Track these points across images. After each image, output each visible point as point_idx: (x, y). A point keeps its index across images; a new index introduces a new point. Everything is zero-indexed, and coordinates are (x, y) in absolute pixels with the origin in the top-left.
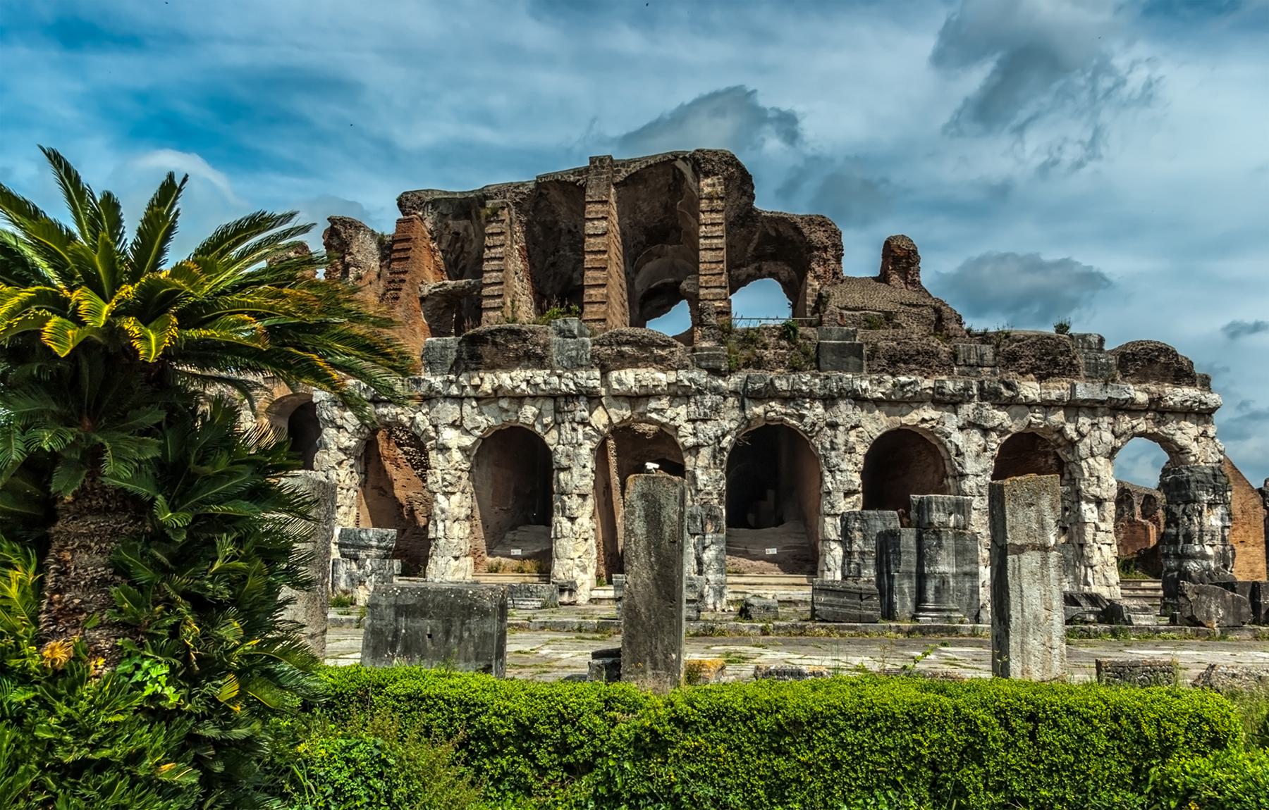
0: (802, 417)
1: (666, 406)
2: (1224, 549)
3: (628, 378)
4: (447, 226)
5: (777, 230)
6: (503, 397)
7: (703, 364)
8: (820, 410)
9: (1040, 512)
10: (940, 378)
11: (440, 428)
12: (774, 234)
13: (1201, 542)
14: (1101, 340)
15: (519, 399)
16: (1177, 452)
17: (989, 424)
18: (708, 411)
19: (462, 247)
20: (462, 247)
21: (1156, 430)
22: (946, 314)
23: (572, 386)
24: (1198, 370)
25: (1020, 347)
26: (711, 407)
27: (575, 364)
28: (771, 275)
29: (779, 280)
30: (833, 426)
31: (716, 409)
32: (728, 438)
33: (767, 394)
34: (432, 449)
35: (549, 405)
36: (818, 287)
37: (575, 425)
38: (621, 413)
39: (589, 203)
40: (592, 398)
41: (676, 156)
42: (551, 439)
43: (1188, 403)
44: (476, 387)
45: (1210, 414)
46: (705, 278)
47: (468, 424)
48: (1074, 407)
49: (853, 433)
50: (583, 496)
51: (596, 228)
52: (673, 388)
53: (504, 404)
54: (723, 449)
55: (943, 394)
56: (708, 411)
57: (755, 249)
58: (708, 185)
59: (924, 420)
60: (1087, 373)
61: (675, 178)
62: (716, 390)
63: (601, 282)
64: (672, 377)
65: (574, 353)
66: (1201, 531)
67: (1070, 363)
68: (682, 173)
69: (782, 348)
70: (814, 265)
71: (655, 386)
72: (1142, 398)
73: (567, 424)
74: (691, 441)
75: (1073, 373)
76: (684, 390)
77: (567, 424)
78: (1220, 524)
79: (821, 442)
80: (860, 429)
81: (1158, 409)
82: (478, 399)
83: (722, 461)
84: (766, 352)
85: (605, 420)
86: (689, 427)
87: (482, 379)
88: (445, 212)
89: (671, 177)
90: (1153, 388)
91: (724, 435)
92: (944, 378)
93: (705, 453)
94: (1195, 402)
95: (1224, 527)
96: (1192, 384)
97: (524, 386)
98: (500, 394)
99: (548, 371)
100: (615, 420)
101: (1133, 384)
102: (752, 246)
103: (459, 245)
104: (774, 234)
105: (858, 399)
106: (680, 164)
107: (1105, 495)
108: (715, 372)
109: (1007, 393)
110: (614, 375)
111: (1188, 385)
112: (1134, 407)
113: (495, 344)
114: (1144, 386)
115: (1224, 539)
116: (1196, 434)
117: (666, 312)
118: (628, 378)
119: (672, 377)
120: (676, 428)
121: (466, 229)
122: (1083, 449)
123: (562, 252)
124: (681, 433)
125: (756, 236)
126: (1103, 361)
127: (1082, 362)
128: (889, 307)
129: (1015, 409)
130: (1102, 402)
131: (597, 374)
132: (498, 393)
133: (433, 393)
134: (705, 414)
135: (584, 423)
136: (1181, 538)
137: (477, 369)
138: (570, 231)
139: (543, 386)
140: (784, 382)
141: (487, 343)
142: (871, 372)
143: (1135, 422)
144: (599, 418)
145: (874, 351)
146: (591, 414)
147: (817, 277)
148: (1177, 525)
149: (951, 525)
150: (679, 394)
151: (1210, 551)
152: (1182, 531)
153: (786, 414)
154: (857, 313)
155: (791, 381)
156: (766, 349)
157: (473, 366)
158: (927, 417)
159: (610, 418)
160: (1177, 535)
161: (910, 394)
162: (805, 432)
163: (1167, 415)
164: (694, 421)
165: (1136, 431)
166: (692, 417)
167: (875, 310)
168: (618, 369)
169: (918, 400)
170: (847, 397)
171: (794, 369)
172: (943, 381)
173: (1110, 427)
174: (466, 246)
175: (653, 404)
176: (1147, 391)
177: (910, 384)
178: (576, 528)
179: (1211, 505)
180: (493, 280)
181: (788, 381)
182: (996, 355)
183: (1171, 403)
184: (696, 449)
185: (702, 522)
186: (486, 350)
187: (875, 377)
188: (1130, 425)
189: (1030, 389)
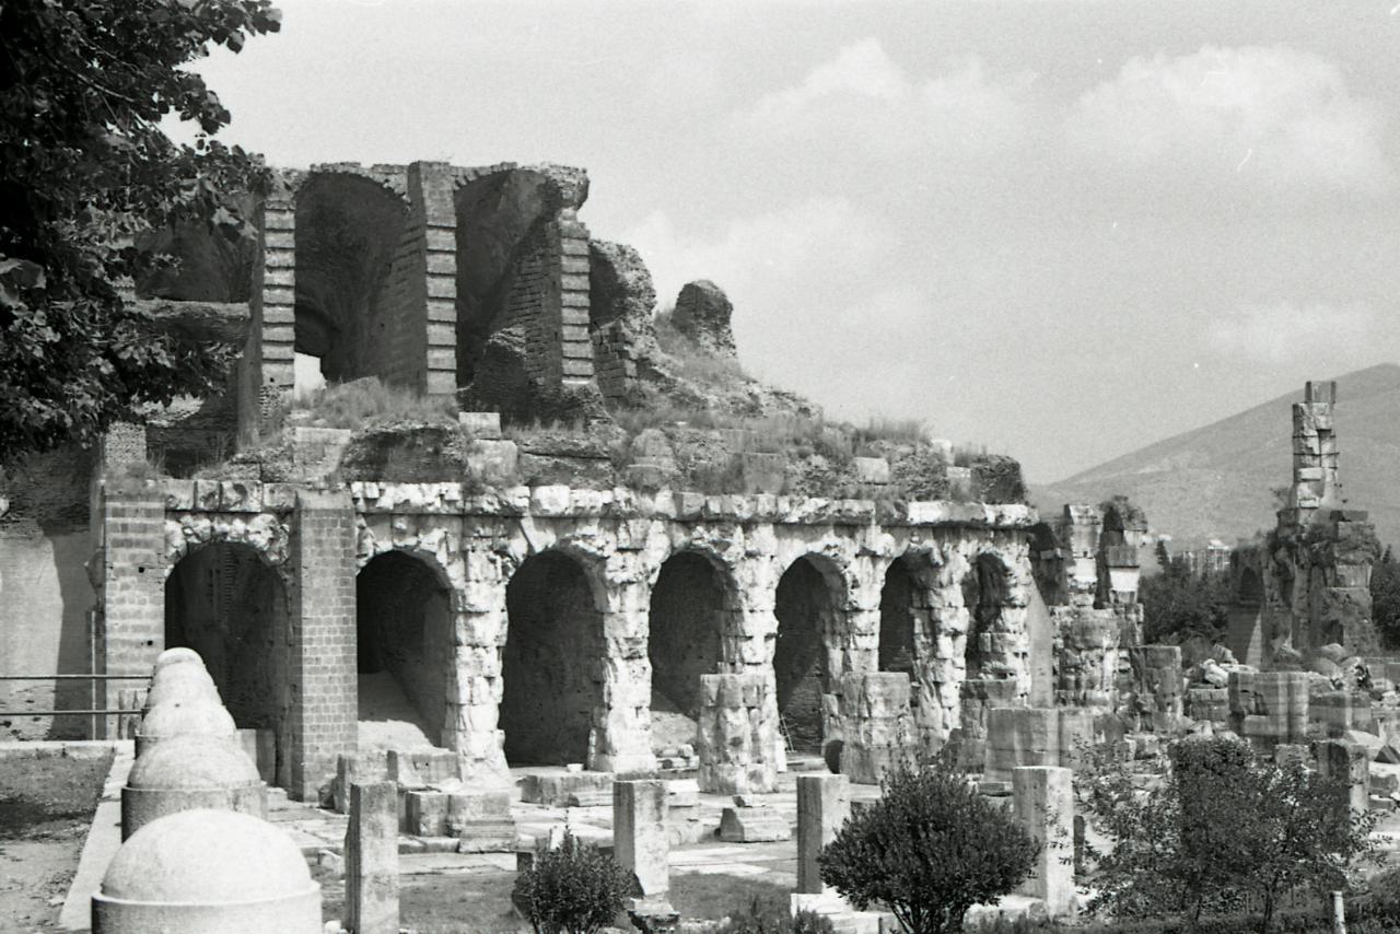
3: (556, 497)
15: (421, 518)
23: (498, 507)
30: (750, 555)
38: (543, 539)
39: (431, 227)
42: (454, 572)
44: (368, 501)
53: (401, 524)
59: (828, 547)
64: (606, 497)
71: (592, 508)
74: (620, 577)
77: (478, 552)
79: (741, 574)
85: (524, 550)
87: (381, 491)
97: (438, 503)
100: (538, 549)
105: (781, 526)
110: (543, 493)
118: (556, 497)
119: (606, 497)
120: (602, 560)
124: (610, 567)
129: (897, 531)
150: (612, 518)
158: (832, 544)
159: (530, 546)
164: (621, 550)
166: (624, 545)
168: (549, 484)
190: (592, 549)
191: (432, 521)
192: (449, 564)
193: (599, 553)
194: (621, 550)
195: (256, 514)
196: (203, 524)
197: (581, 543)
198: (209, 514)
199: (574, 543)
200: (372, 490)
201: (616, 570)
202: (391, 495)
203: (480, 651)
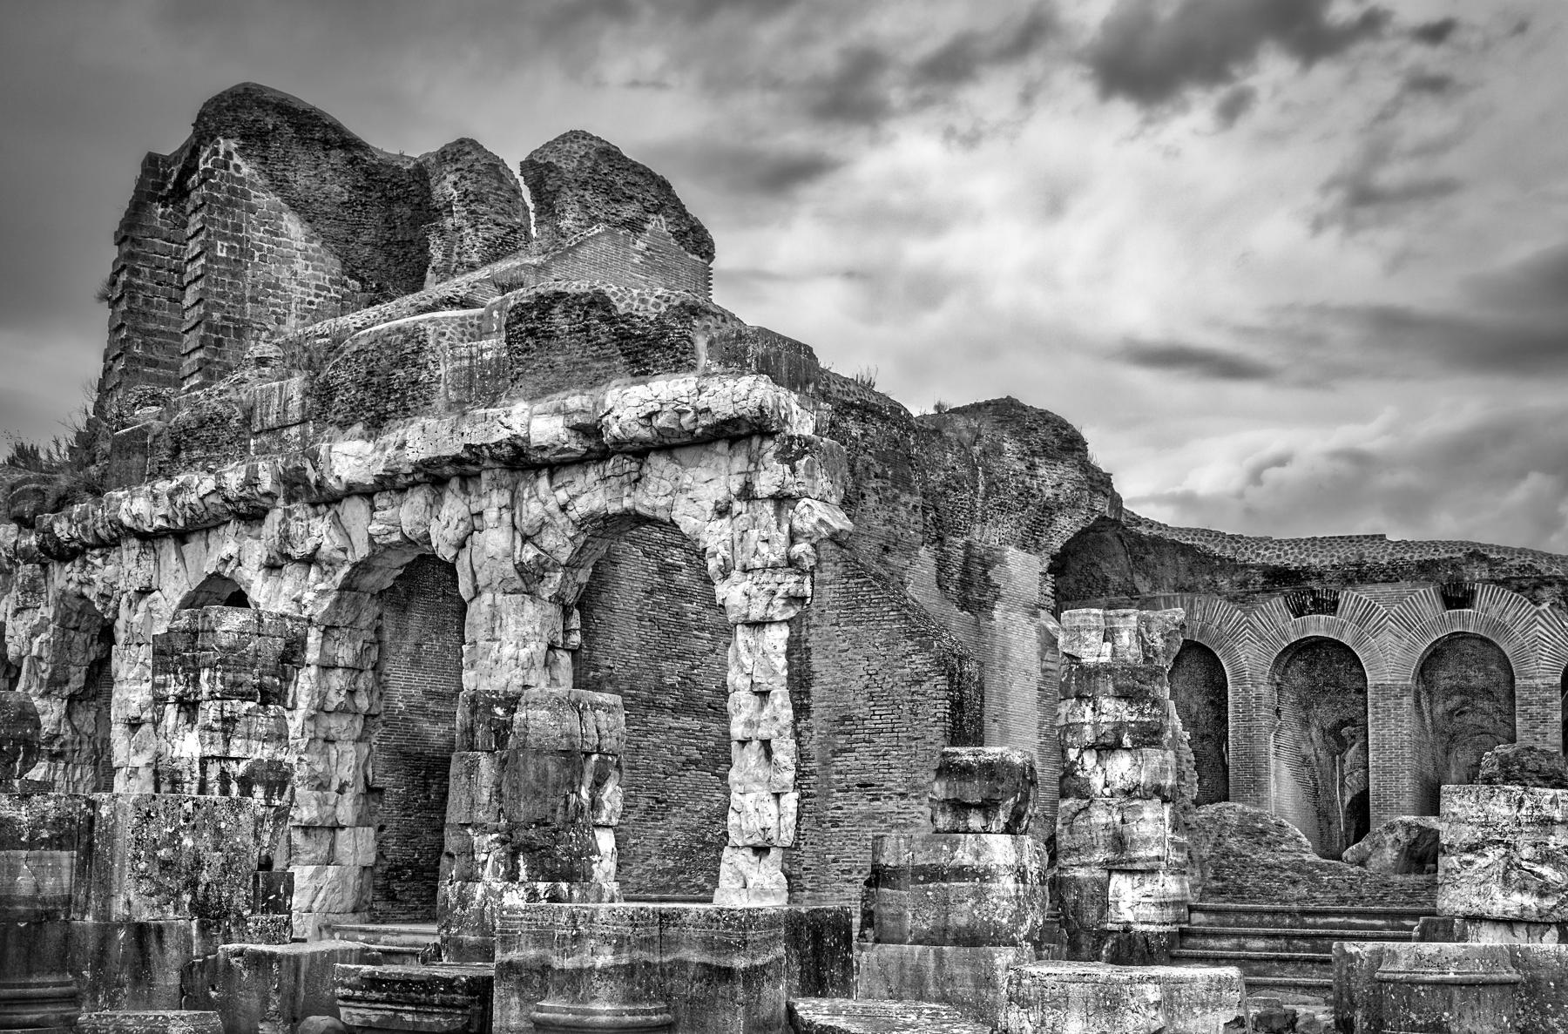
21: (627, 503)
32: (44, 636)
49: (142, 605)
80: (157, 594)
90: (575, 401)
94: (681, 413)
101: (533, 398)
111: (666, 368)
116: (721, 495)
126: (487, 356)
143: (562, 496)
163: (652, 458)
165: (574, 515)
173: (507, 516)
176: (558, 411)
183: (615, 430)
188: (552, 507)
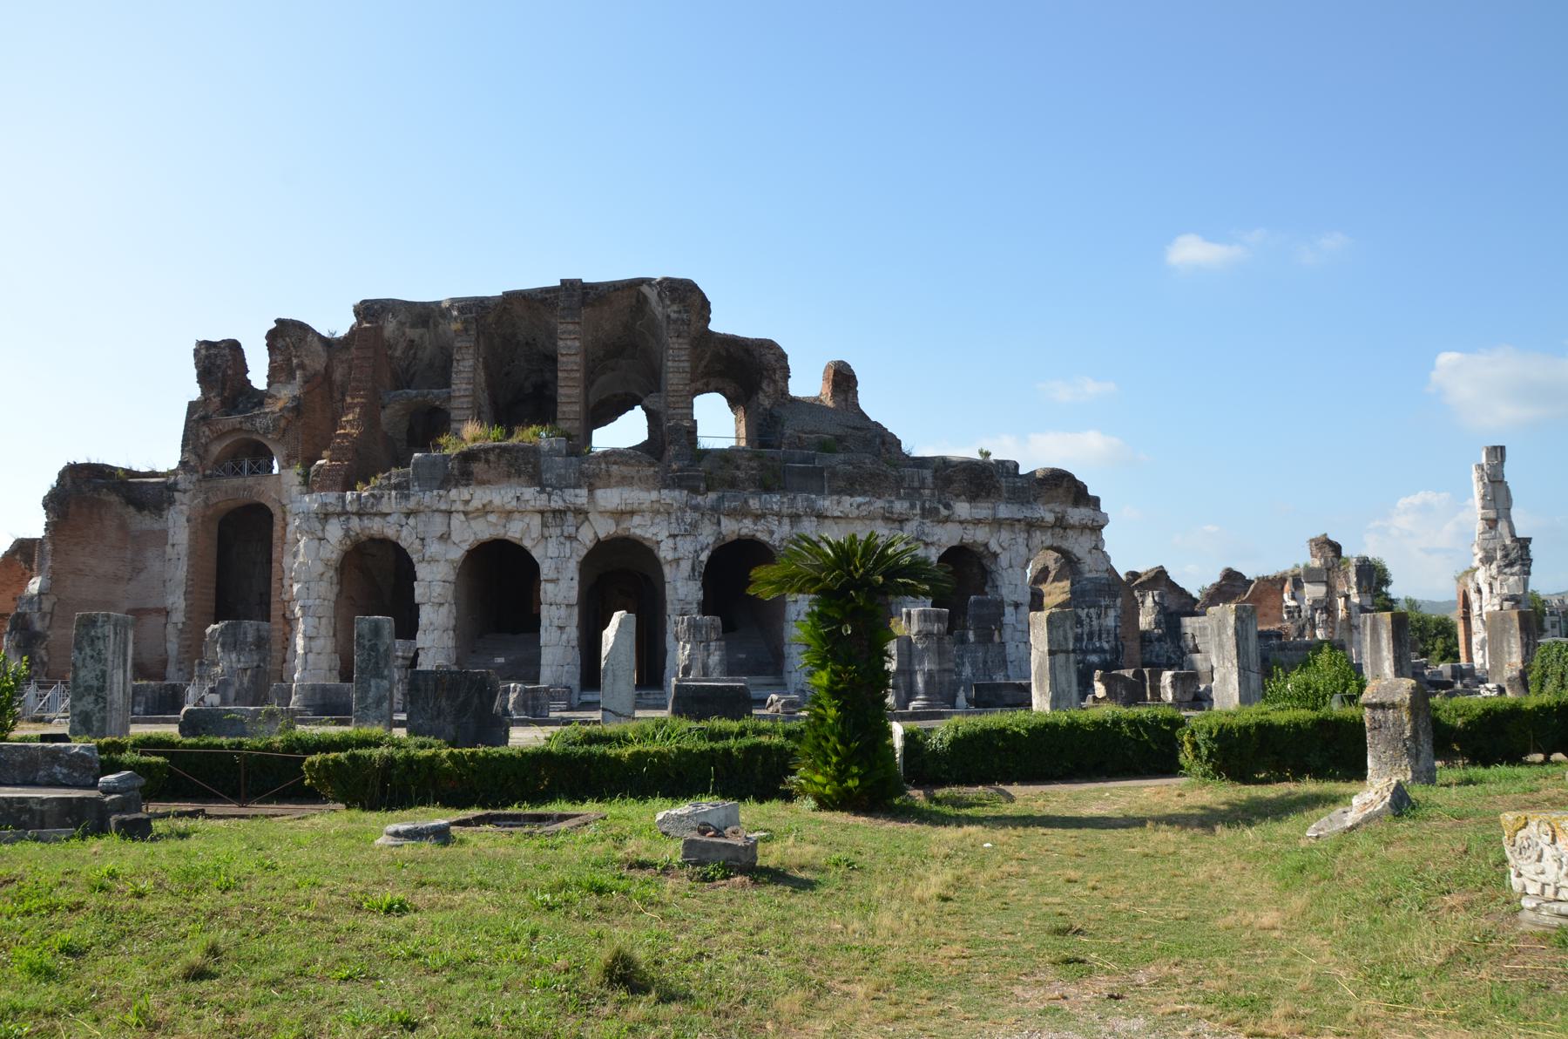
0: (772, 533)
1: (649, 523)
2: (1116, 645)
4: (404, 334)
5: (727, 351)
6: (492, 512)
7: (683, 484)
8: (786, 528)
9: (1065, 631)
10: (889, 498)
11: (428, 541)
12: (724, 354)
13: (1100, 638)
14: (1017, 466)
16: (1076, 563)
17: (929, 540)
18: (688, 527)
19: (415, 353)
20: (415, 353)
22: (887, 439)
24: (1091, 492)
25: (955, 472)
26: (690, 524)
27: (562, 485)
28: (717, 390)
29: (724, 394)
31: (694, 525)
33: (740, 513)
34: (419, 561)
35: (537, 519)
36: (768, 407)
37: (562, 539)
38: (605, 528)
40: (582, 514)
41: (642, 281)
43: (1084, 522)
44: (467, 502)
45: (1100, 530)
46: (673, 399)
47: (455, 537)
48: (997, 523)
50: (572, 605)
51: (569, 348)
52: (656, 506)
53: (492, 518)
54: (702, 562)
55: (892, 513)
56: (688, 527)
57: (705, 367)
58: (675, 312)
60: (1006, 495)
61: (638, 301)
62: (695, 508)
63: (573, 400)
64: (654, 495)
65: (563, 471)
66: (1100, 630)
67: (994, 487)
68: (645, 297)
69: (752, 469)
70: (764, 386)
72: (1050, 518)
73: (554, 539)
74: (670, 557)
75: (996, 496)
76: (666, 506)
77: (554, 539)
78: (1113, 624)
81: (1061, 524)
82: (463, 512)
83: (700, 572)
84: (738, 473)
85: (591, 536)
86: (671, 542)
88: (403, 321)
89: (634, 300)
91: (702, 550)
92: (893, 498)
93: (686, 566)
95: (1116, 627)
96: (1087, 505)
97: (514, 503)
98: (488, 508)
99: (538, 489)
100: (602, 535)
101: (1043, 504)
102: (704, 363)
103: (412, 352)
104: (724, 354)
105: (821, 516)
106: (645, 289)
107: (1020, 599)
108: (694, 490)
109: (944, 512)
110: (599, 493)
112: (1043, 524)
113: (487, 461)
114: (1051, 506)
115: (1116, 635)
117: (612, 421)
120: (658, 543)
121: (421, 337)
122: (1004, 560)
123: (516, 362)
125: (708, 355)
126: (1019, 484)
127: (1004, 484)
128: (839, 432)
130: (1019, 521)
131: (584, 492)
132: (485, 511)
133: (422, 508)
134: (686, 530)
135: (570, 538)
136: (1085, 636)
137: (467, 485)
138: (527, 343)
139: (532, 503)
140: (757, 501)
141: (480, 461)
142: (832, 493)
144: (587, 536)
145: (834, 475)
146: (577, 529)
147: (768, 397)
148: (1082, 626)
149: (935, 632)
151: (1106, 646)
152: (1086, 629)
153: (757, 531)
154: (812, 436)
155: (763, 500)
156: (738, 469)
157: (464, 482)
159: (595, 533)
160: (1082, 634)
161: (864, 513)
162: (774, 546)
164: (674, 536)
167: (827, 434)
168: (607, 486)
169: (871, 517)
170: (812, 515)
171: (767, 489)
172: (892, 502)
174: (420, 353)
175: (637, 520)
176: (1051, 511)
177: (864, 504)
178: (564, 637)
179: (1107, 607)
180: (462, 393)
181: (760, 501)
182: (935, 477)
184: (677, 561)
185: (706, 632)
186: (478, 468)
187: (835, 497)
189: (962, 509)
190: (648, 535)
191: (517, 515)
192: (534, 546)
193: (654, 538)
194: (674, 536)
195: (389, 514)
196: (355, 523)
197: (638, 532)
198: (360, 515)
199: (632, 530)
200: (465, 493)
201: (665, 553)
202: (480, 496)
203: (554, 607)
